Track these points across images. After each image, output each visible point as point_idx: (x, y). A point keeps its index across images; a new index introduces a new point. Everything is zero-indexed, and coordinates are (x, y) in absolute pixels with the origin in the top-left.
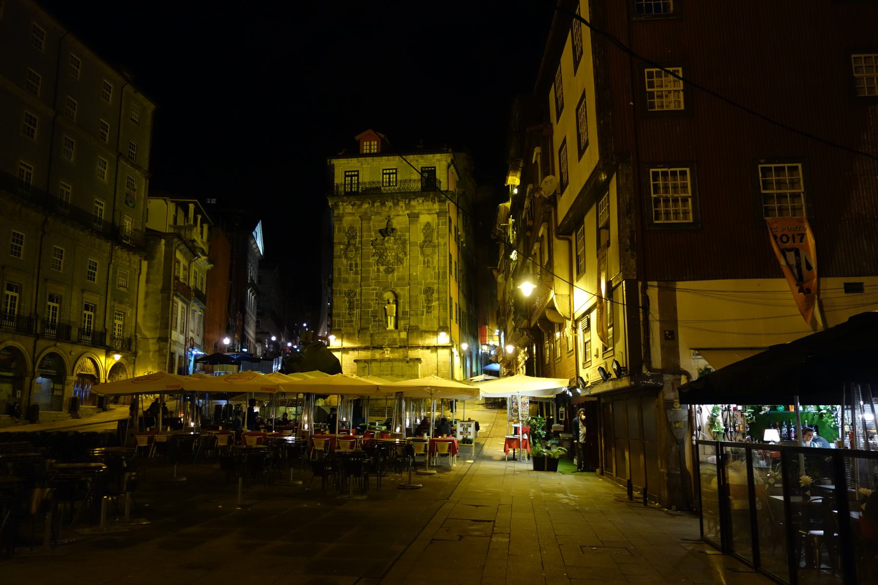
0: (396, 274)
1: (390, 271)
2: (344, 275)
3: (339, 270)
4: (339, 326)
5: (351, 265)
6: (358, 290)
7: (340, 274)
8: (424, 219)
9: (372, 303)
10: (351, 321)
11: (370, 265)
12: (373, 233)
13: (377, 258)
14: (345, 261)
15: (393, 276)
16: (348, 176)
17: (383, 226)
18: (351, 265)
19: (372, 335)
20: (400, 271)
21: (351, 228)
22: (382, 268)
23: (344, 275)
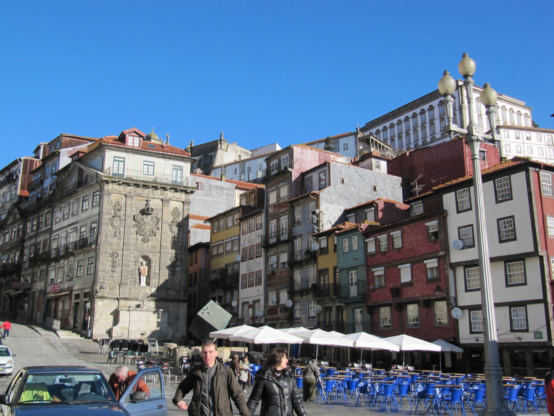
0: (150, 243)
1: (145, 240)
2: (109, 239)
3: (106, 234)
4: (103, 279)
5: (116, 232)
6: (120, 253)
7: (106, 238)
8: (173, 204)
9: (131, 263)
10: (114, 277)
11: (131, 234)
12: (134, 209)
13: (136, 229)
14: (110, 228)
15: (148, 244)
16: (116, 161)
17: (142, 206)
18: (116, 232)
19: (130, 289)
20: (154, 242)
21: (118, 203)
22: (140, 238)
23: (109, 239)
